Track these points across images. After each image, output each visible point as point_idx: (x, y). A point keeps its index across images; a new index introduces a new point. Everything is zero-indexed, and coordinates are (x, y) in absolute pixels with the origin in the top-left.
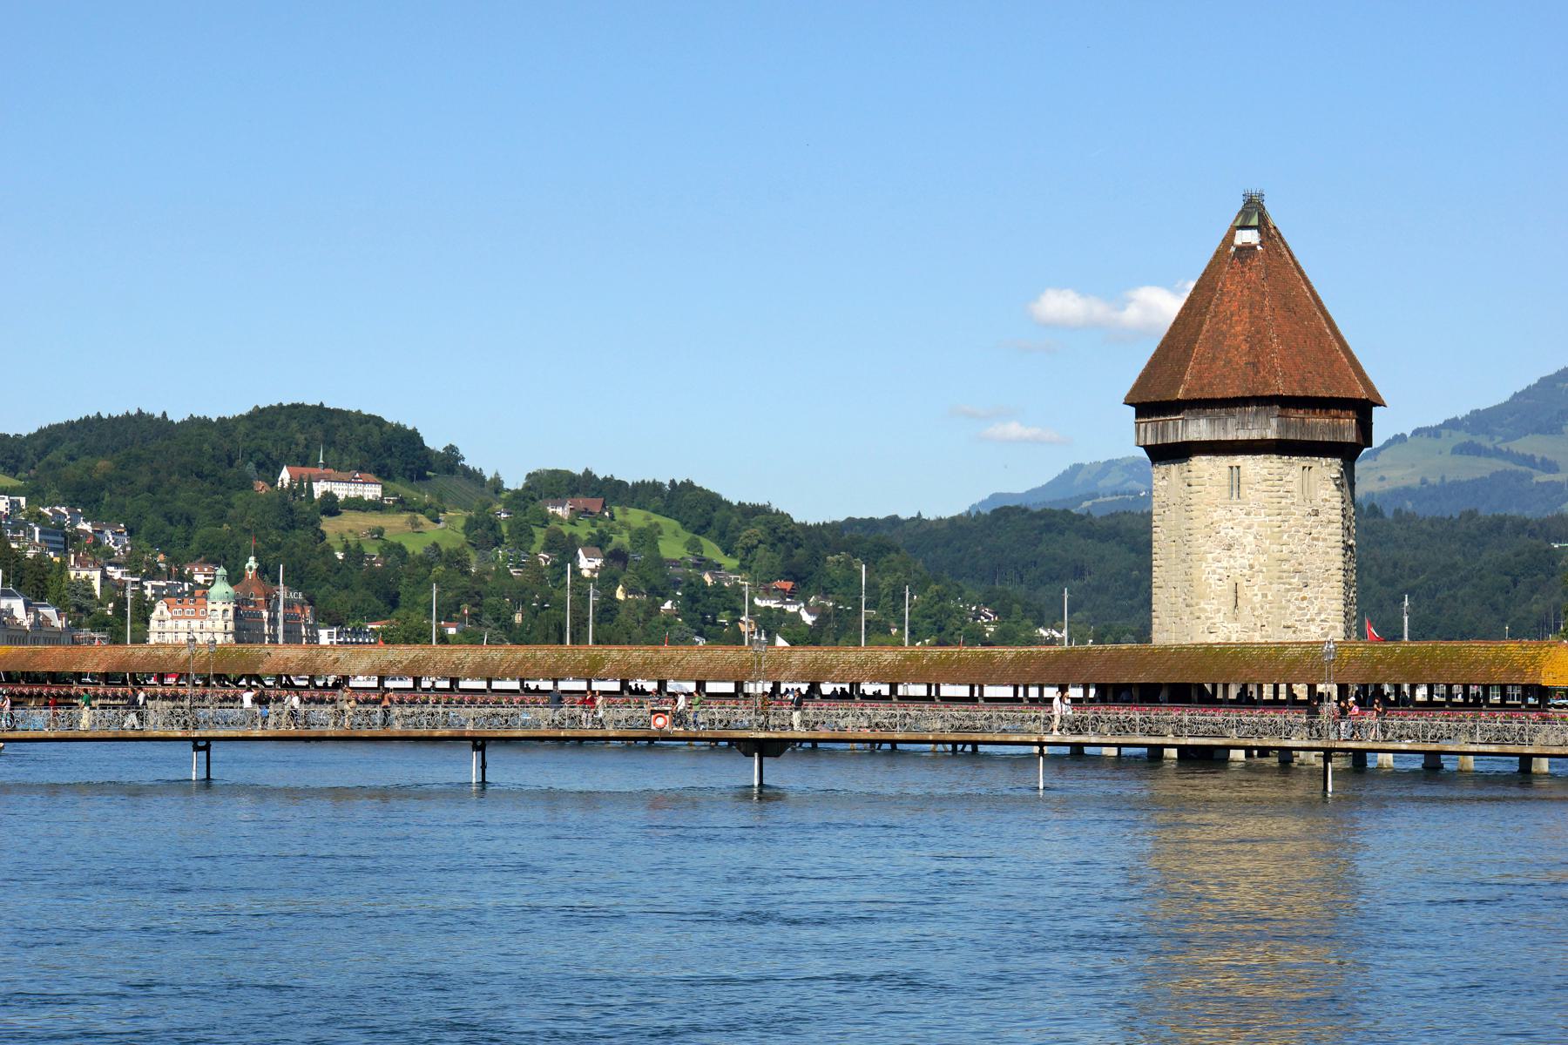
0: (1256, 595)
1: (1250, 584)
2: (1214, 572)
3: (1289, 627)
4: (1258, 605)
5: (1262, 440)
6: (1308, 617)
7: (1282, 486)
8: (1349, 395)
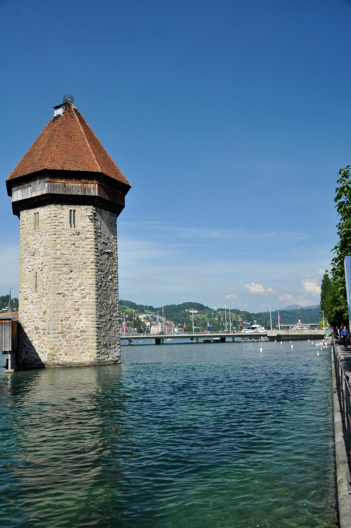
0: (44, 278)
1: (42, 272)
2: (27, 268)
3: (60, 294)
4: (45, 283)
5: (43, 196)
6: (73, 288)
7: (56, 220)
8: (90, 170)
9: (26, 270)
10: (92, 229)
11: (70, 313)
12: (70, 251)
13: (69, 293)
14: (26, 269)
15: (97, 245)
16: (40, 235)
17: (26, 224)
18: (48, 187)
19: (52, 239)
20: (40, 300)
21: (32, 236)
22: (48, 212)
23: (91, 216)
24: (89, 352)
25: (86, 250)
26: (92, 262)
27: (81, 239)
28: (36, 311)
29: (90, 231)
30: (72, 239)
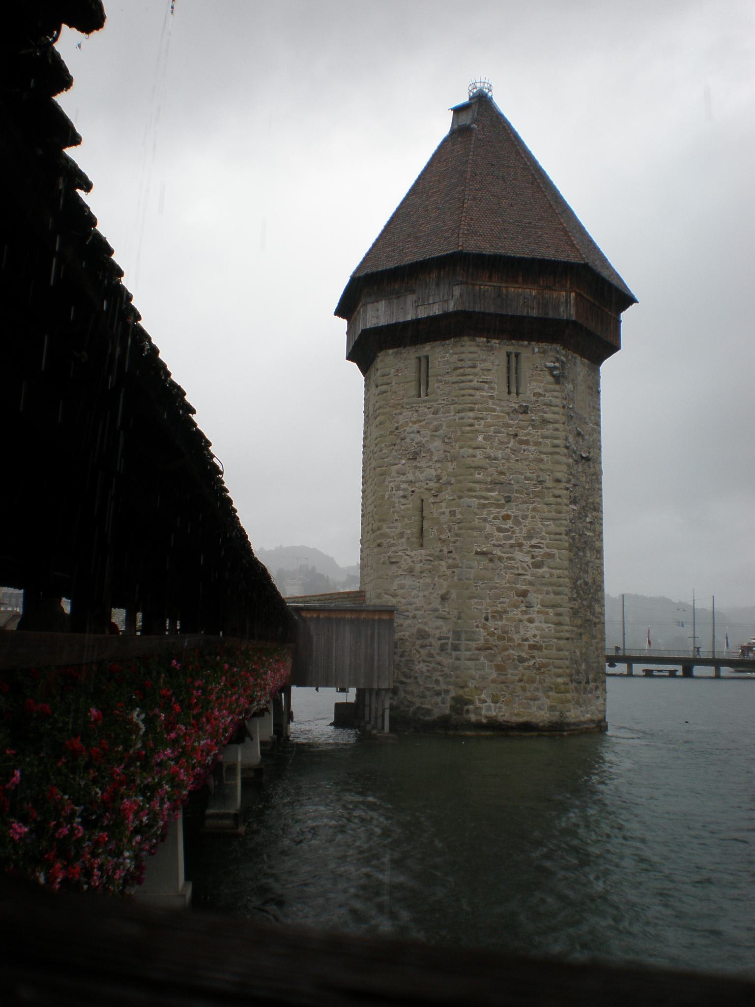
4: (445, 526)
5: (446, 316)
7: (475, 374)
9: (394, 492)
10: (557, 400)
11: (507, 601)
12: (506, 451)
13: (504, 553)
14: (394, 489)
15: (566, 439)
16: (432, 410)
17: (394, 383)
18: (461, 295)
19: (464, 421)
20: (431, 566)
21: (410, 413)
22: (456, 356)
23: (555, 368)
24: (548, 697)
25: (545, 450)
26: (558, 481)
27: (533, 423)
28: (421, 594)
29: (552, 404)
30: (511, 422)
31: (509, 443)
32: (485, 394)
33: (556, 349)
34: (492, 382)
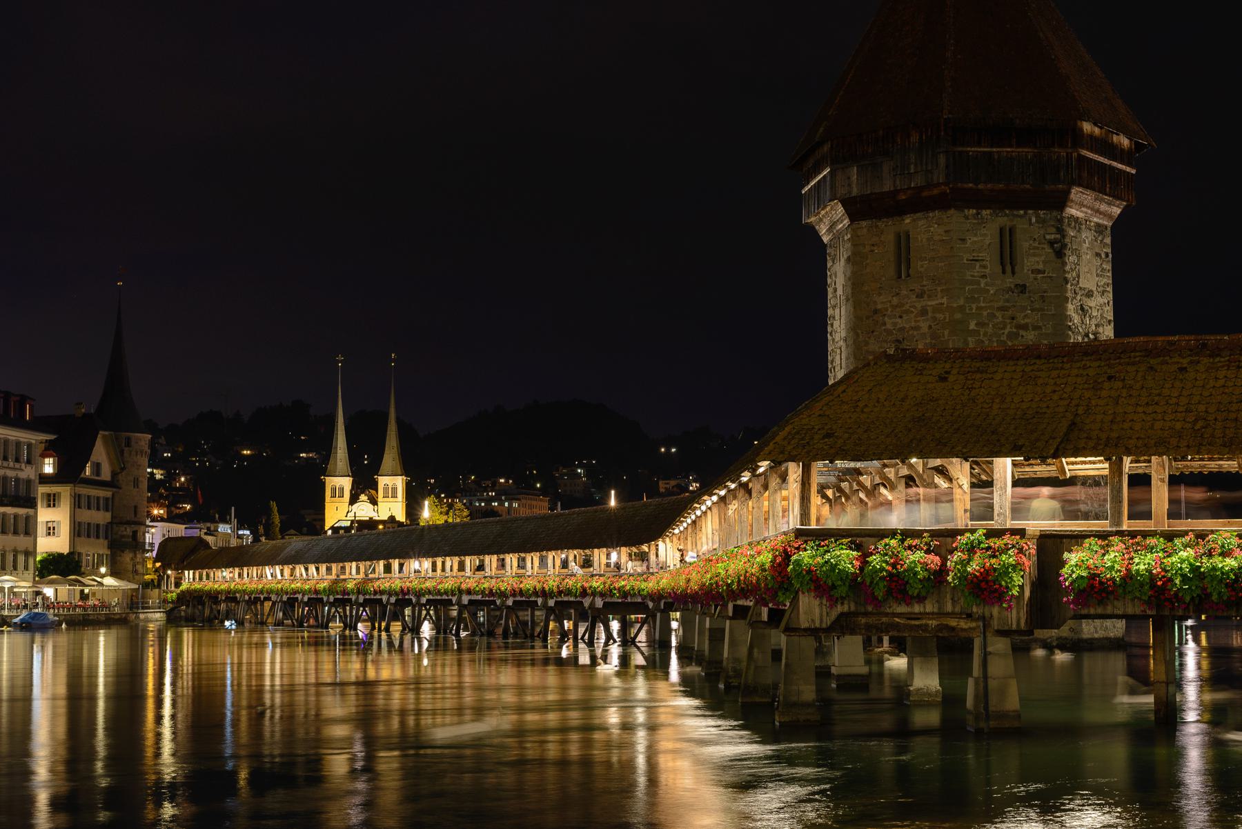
18: (947, 167)
31: (1004, 328)
32: (976, 274)
33: (1057, 216)
34: (983, 260)
